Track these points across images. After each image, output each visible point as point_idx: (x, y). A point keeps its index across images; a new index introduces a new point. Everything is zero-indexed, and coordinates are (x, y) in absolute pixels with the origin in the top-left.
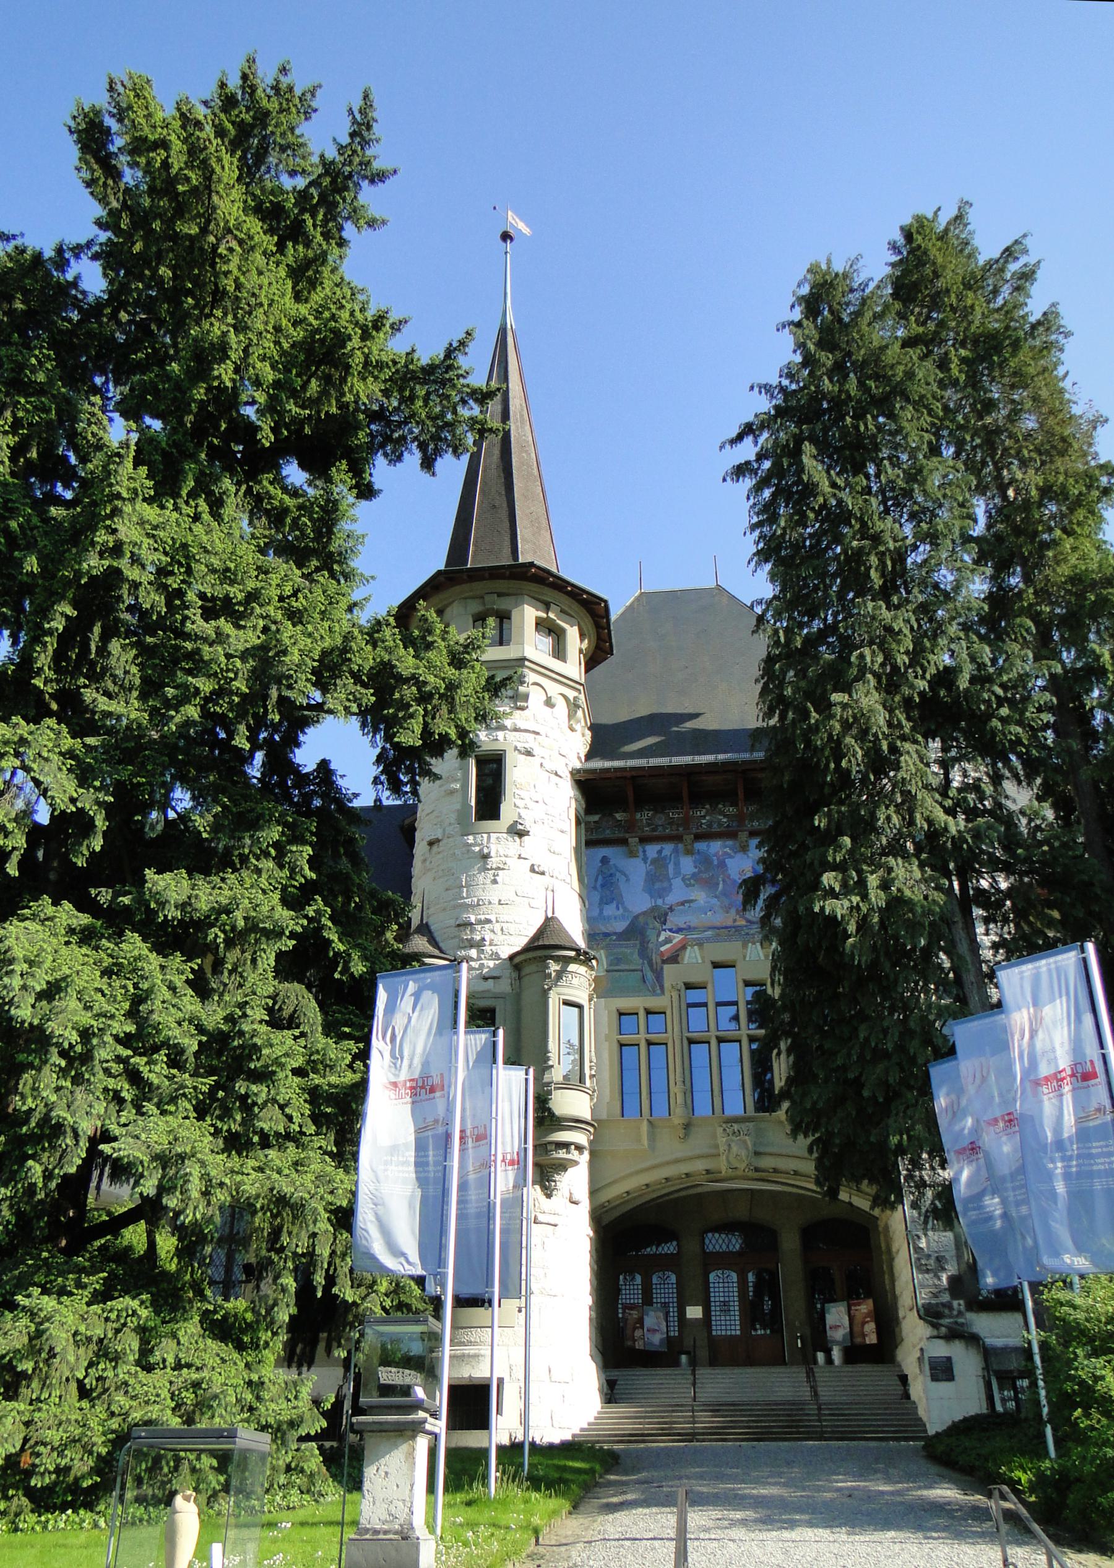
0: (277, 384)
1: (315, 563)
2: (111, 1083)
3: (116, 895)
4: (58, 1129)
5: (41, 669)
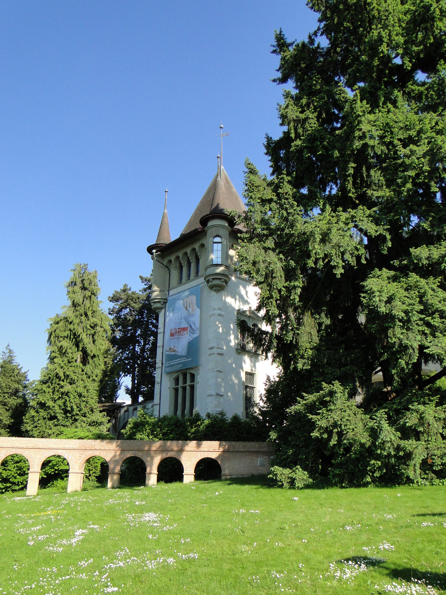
0: (406, 42)
1: (441, 108)
2: (420, 328)
3: (401, 261)
4: (406, 347)
5: (350, 190)
